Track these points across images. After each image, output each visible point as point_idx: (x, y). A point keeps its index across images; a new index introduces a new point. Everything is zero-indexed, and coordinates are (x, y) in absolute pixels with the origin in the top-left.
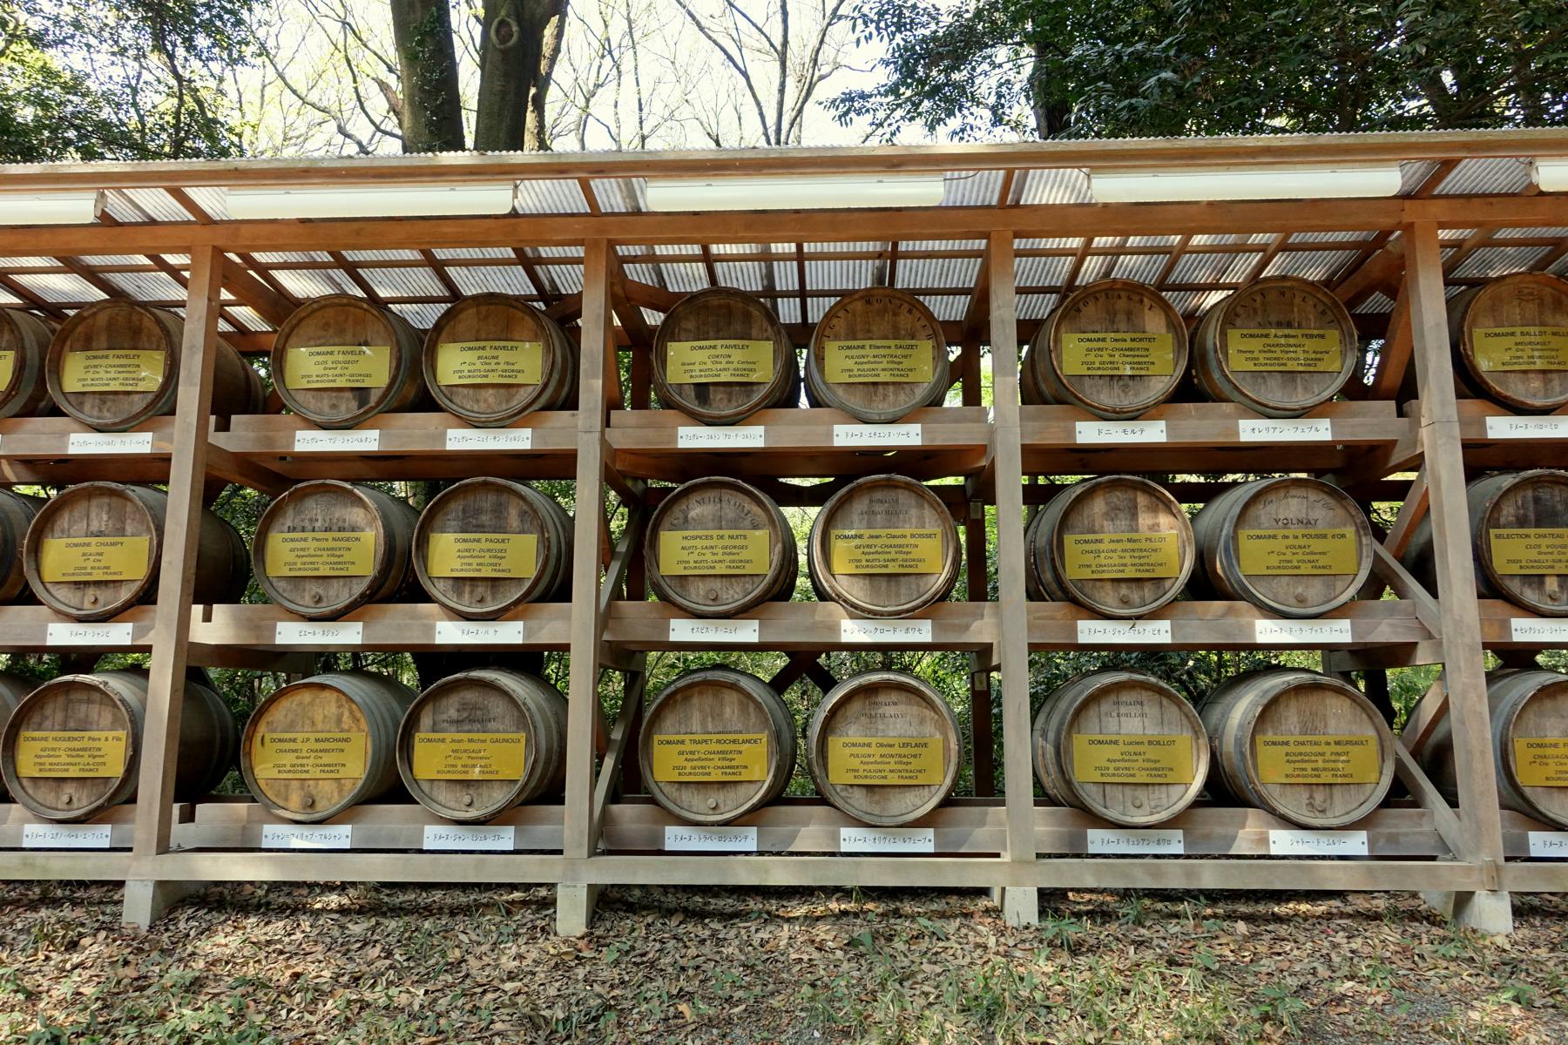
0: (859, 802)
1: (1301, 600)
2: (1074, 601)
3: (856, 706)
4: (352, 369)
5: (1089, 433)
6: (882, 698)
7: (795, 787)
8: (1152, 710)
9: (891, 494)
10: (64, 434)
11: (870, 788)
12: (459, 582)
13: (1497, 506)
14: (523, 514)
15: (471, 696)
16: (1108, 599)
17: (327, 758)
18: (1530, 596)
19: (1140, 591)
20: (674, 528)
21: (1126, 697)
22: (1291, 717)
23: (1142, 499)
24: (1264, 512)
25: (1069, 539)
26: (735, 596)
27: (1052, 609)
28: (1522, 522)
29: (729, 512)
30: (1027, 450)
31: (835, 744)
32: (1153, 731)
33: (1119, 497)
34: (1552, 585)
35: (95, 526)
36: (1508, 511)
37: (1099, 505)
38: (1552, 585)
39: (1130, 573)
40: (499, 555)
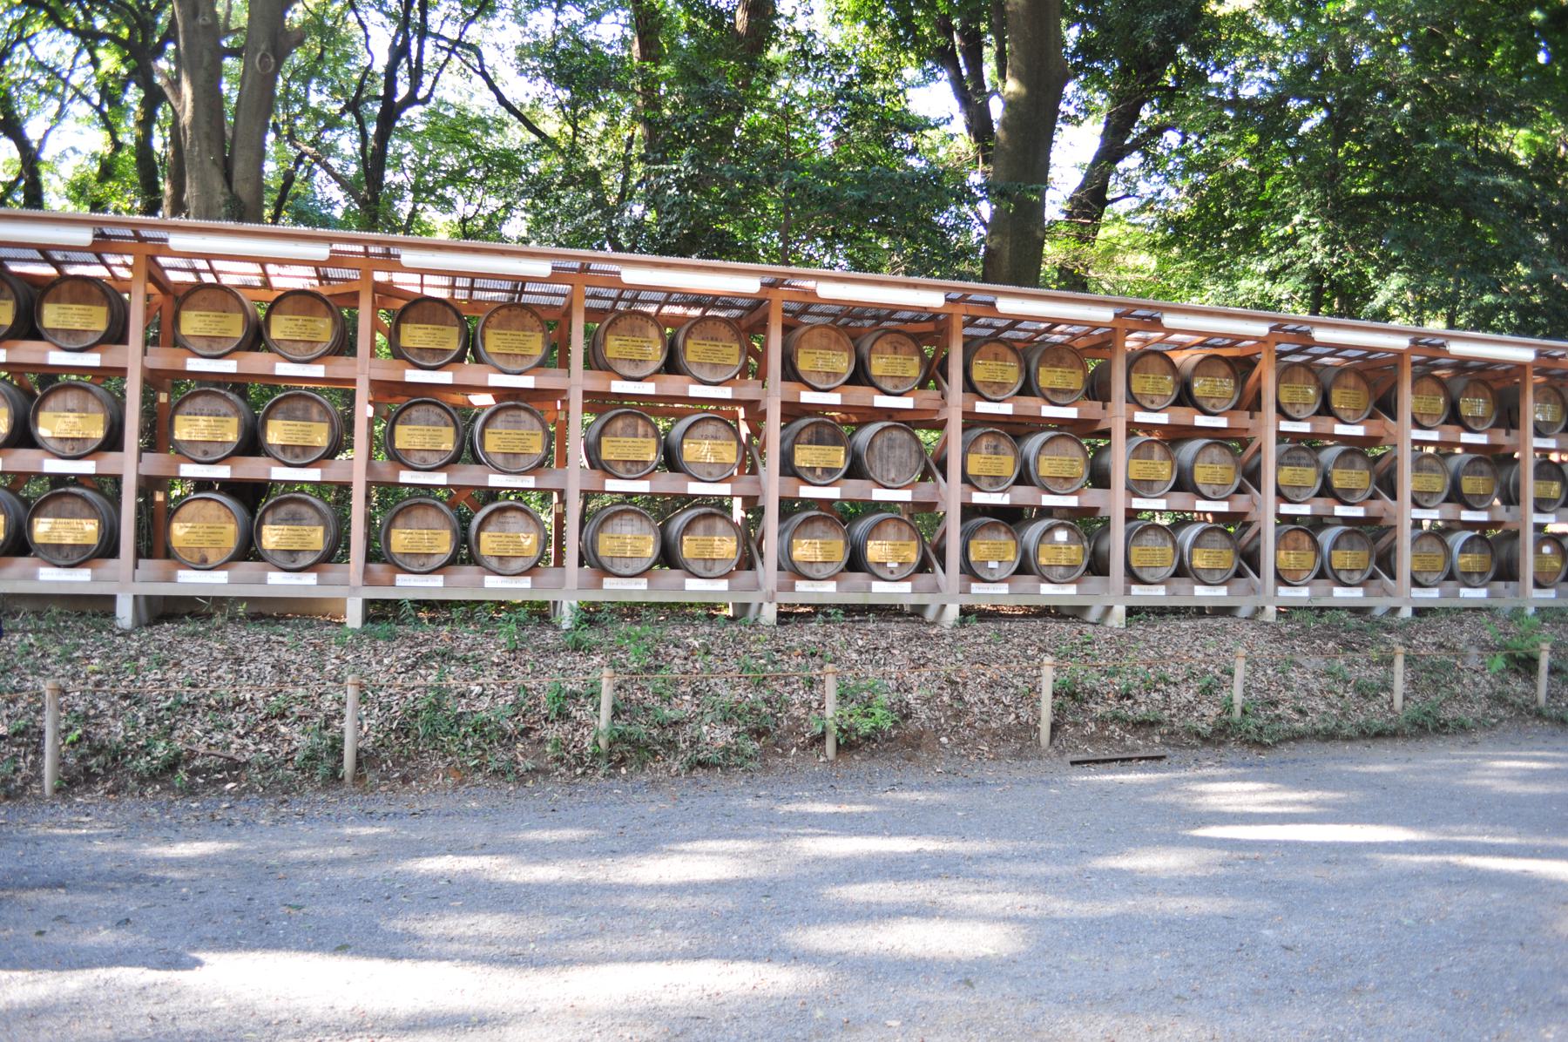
0: (494, 564)
1: (710, 474)
2: (605, 470)
3: (494, 518)
4: (221, 326)
5: (618, 387)
6: (509, 514)
7: (465, 554)
8: (637, 522)
9: (517, 413)
10: (46, 352)
11: (500, 557)
12: (284, 448)
13: (799, 434)
14: (320, 413)
15: (292, 507)
16: (620, 470)
17: (214, 537)
18: (809, 477)
19: (637, 469)
20: (403, 423)
21: (627, 517)
22: (700, 527)
23: (640, 422)
24: (696, 432)
25: (604, 440)
26: (435, 461)
27: (597, 474)
28: (810, 443)
29: (434, 418)
30: (586, 394)
31: (483, 535)
32: (636, 534)
33: (629, 420)
34: (819, 472)
35: (70, 405)
36: (804, 436)
37: (619, 424)
38: (819, 472)
39: (632, 458)
40: (308, 433)
